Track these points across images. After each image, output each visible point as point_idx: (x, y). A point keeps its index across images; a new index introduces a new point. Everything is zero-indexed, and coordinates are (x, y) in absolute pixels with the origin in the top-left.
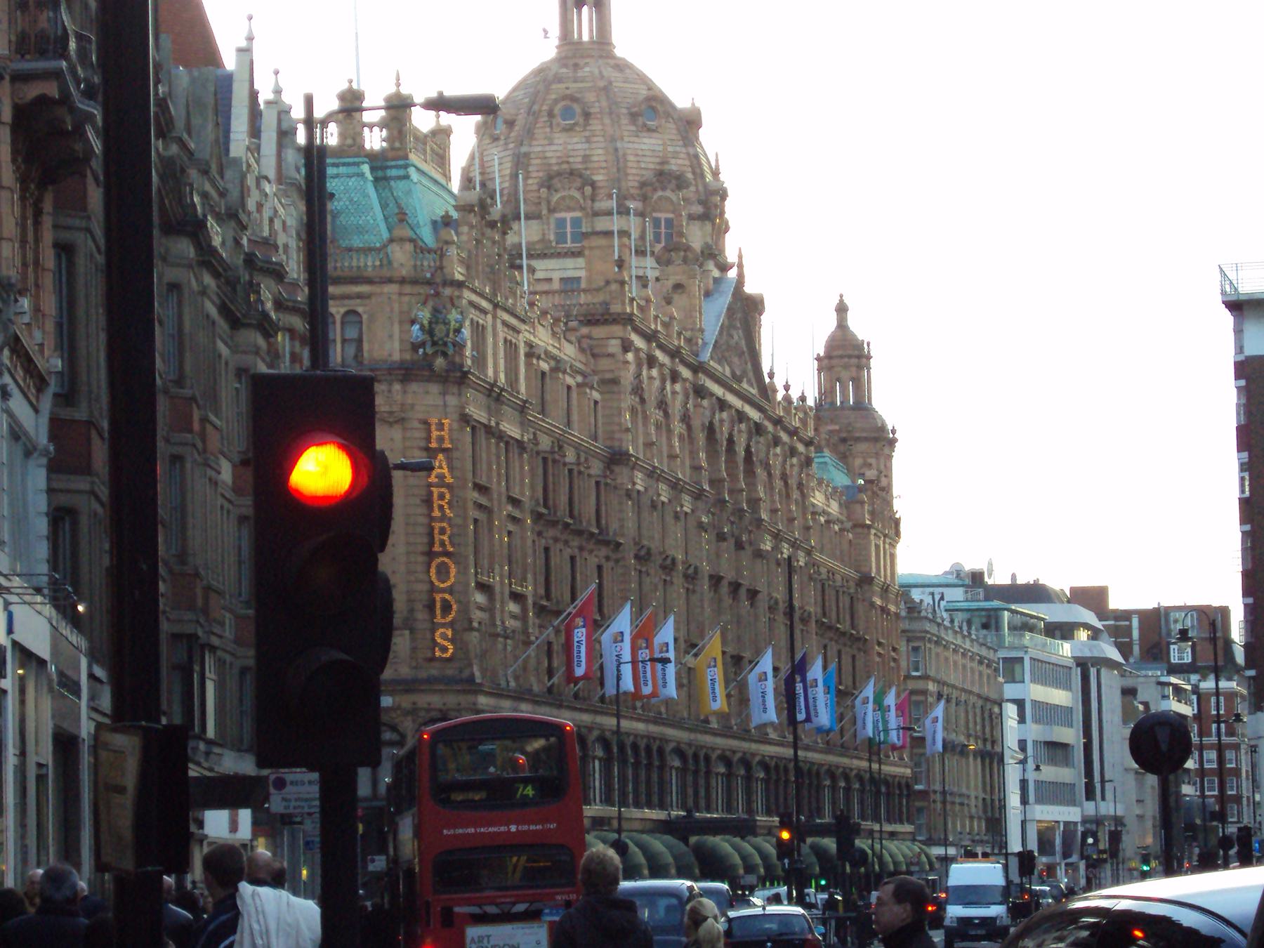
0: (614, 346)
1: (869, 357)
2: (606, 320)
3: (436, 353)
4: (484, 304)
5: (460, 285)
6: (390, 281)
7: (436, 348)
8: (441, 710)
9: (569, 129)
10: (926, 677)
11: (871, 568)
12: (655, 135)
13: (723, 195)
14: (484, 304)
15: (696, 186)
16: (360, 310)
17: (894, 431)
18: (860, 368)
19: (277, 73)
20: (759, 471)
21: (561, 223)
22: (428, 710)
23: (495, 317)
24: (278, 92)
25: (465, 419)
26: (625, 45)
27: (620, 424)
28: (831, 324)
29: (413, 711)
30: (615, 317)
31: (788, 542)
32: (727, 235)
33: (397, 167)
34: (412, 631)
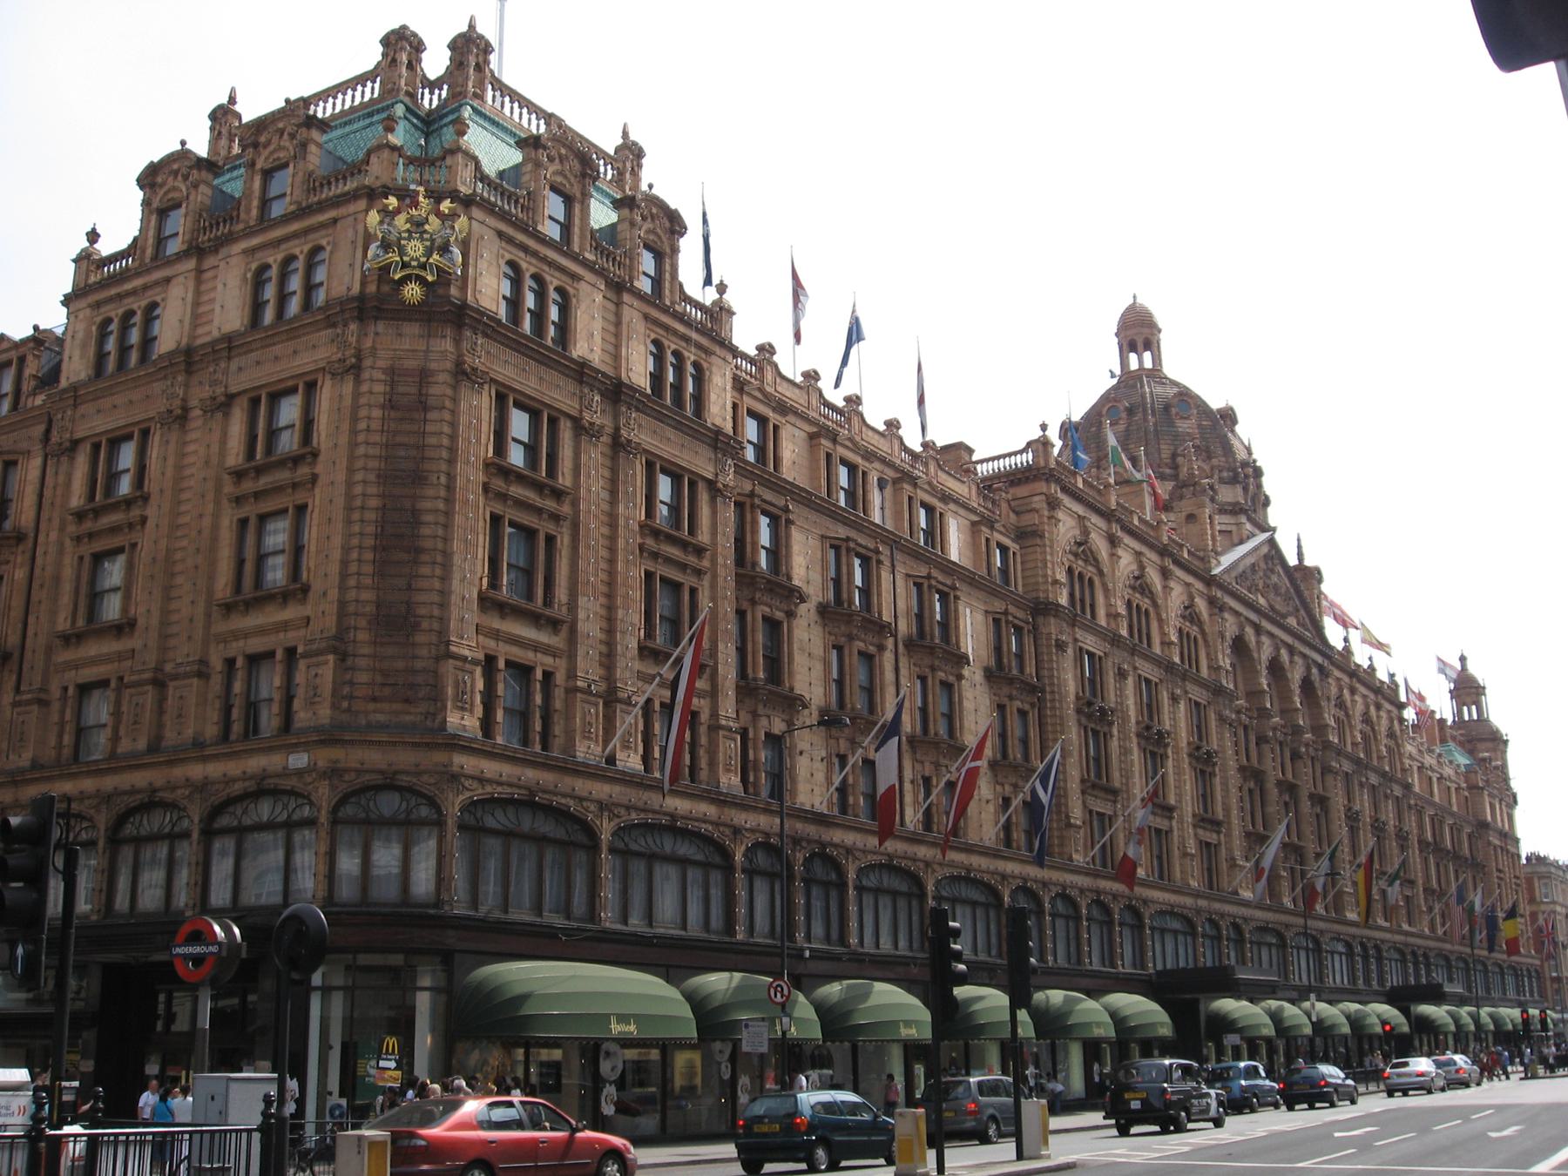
0: (1039, 502)
2: (1027, 478)
3: (405, 280)
7: (407, 272)
8: (381, 772)
10: (1554, 902)
13: (1258, 473)
16: (324, 242)
20: (1324, 703)
22: (357, 771)
25: (463, 374)
26: (1171, 369)
27: (1045, 576)
29: (334, 772)
30: (1035, 473)
33: (452, 111)
34: (343, 657)
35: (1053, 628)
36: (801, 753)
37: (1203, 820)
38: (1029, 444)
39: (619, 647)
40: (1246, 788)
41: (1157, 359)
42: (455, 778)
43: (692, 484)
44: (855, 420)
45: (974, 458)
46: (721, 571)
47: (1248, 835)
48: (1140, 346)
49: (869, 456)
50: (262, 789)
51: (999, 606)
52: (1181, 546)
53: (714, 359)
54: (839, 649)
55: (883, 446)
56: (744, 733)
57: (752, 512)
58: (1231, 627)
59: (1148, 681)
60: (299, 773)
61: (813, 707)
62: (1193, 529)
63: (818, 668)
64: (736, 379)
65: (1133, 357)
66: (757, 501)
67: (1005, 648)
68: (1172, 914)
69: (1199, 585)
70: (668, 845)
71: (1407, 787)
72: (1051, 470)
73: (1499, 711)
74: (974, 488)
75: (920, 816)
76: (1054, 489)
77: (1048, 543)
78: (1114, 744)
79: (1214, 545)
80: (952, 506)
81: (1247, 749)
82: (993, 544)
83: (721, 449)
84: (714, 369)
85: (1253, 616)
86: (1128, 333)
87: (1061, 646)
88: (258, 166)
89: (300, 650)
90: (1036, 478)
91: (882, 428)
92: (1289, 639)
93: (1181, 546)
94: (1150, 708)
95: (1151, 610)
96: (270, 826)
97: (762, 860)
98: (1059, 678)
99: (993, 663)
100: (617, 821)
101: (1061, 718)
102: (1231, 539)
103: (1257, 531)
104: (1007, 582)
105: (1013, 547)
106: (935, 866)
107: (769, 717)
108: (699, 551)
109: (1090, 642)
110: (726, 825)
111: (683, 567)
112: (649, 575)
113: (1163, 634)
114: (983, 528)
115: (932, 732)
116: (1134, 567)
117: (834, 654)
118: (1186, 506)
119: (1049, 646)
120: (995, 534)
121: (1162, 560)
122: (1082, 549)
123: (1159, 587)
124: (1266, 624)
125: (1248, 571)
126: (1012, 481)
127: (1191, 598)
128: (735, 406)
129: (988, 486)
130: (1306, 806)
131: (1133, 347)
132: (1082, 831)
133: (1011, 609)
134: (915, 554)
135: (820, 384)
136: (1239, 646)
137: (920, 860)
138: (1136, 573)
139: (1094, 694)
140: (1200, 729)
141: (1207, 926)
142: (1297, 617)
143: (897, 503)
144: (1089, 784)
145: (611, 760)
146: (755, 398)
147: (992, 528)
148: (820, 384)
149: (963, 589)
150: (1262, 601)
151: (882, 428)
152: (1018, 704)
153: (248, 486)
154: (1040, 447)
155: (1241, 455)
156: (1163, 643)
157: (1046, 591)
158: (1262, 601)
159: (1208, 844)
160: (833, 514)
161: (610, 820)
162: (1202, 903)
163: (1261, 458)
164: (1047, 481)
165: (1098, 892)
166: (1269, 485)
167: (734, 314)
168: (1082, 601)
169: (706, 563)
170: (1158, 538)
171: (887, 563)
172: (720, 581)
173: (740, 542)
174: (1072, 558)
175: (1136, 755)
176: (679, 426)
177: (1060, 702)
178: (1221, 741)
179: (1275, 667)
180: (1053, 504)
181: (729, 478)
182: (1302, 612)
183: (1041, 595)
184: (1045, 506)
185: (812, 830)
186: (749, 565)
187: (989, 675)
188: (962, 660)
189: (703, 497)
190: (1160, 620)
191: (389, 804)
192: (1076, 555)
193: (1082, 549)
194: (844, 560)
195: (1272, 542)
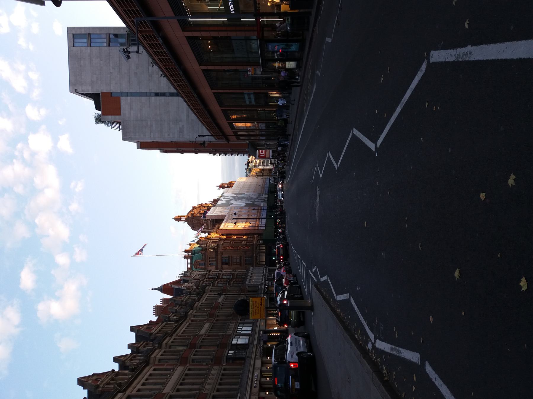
4: (209, 241)
5: (207, 245)
6: (206, 254)
9: (194, 221)
14: (209, 241)
19: (176, 277)
21: (205, 222)
23: (211, 239)
24: (179, 277)
25: (222, 245)
42: (256, 244)
50: (256, 259)
60: (255, 255)
88: (199, 267)
89: (245, 256)
96: (259, 258)
131: (181, 219)
153: (230, 264)
191: (258, 248)
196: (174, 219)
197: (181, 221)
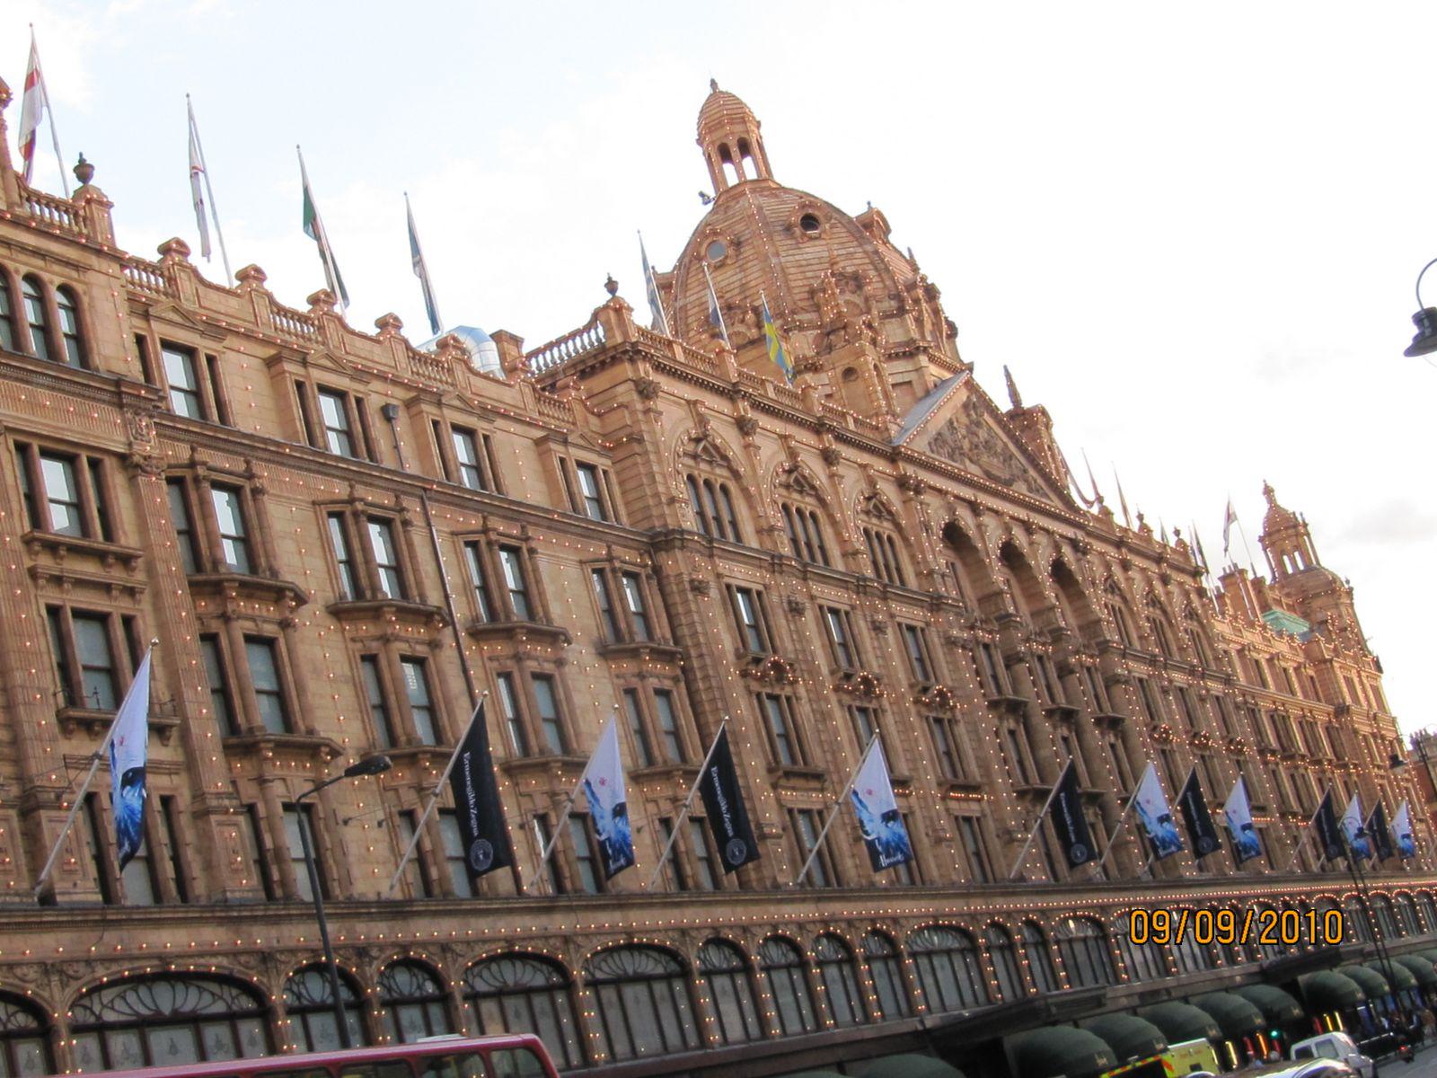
0: (626, 393)
1: (1305, 525)
2: (603, 363)
11: (1344, 700)
12: (817, 243)
13: (932, 293)
15: (883, 281)
17: (1348, 582)
18: (1298, 535)
20: (1089, 591)
26: (785, 175)
27: (657, 495)
28: (1263, 508)
30: (612, 353)
31: (1180, 669)
32: (959, 341)
35: (675, 563)
36: (346, 822)
37: (954, 788)
38: (596, 316)
39: (26, 727)
40: (1004, 732)
41: (763, 164)
43: (95, 465)
44: (331, 328)
45: (526, 349)
46: (165, 584)
47: (1022, 794)
48: (735, 151)
49: (361, 374)
51: (598, 550)
52: (844, 415)
53: (91, 277)
54: (371, 659)
55: (379, 357)
56: (251, 810)
57: (198, 488)
58: (937, 515)
59: (835, 612)
61: (351, 752)
62: (857, 387)
63: (347, 691)
64: (132, 299)
65: (728, 168)
66: (201, 471)
67: (618, 609)
68: (511, 956)
69: (881, 465)
70: (166, 999)
71: (1228, 681)
72: (634, 345)
73: (1333, 556)
74: (527, 391)
75: (544, 871)
76: (644, 369)
77: (650, 448)
78: (804, 709)
79: (889, 405)
80: (500, 423)
81: (995, 677)
82: (572, 465)
83: (130, 406)
84: (96, 292)
85: (967, 493)
86: (718, 135)
87: (699, 588)
90: (615, 360)
91: (373, 331)
92: (1022, 514)
93: (844, 415)
94: (849, 646)
95: (819, 512)
97: (316, 989)
98: (705, 634)
99: (607, 631)
100: (74, 985)
101: (721, 688)
102: (914, 394)
103: (947, 375)
104: (604, 516)
105: (602, 463)
106: (580, 940)
107: (284, 780)
108: (126, 560)
109: (740, 574)
110: (245, 952)
111: (106, 588)
112: (54, 612)
113: (842, 541)
114: (553, 446)
115: (536, 749)
116: (782, 457)
117: (366, 672)
118: (841, 359)
119: (682, 592)
120: (572, 450)
121: (821, 441)
122: (704, 447)
123: (824, 479)
124: (984, 499)
125: (947, 433)
126: (583, 372)
127: (872, 483)
128: (140, 340)
129: (549, 384)
130: (1095, 737)
131: (725, 155)
132: (784, 841)
133: (618, 551)
134: (457, 499)
135: (267, 285)
136: (954, 535)
137: (555, 936)
138: (787, 466)
139: (762, 647)
140: (924, 662)
141: (992, 934)
142: (1026, 481)
143: (418, 435)
144: (780, 773)
145: (47, 900)
146: (170, 322)
147: (565, 442)
148: (267, 285)
149: (539, 536)
150: (973, 469)
151: (373, 331)
152: (653, 682)
154: (612, 314)
155: (903, 274)
156: (844, 555)
157: (663, 516)
158: (974, 469)
159: (968, 820)
160: (321, 464)
161: (64, 986)
162: (978, 905)
163: (931, 271)
164: (632, 360)
165: (825, 922)
166: (950, 306)
167: (109, 205)
168: (718, 519)
169: (140, 576)
170: (809, 411)
171: (418, 521)
172: (168, 601)
173: (189, 534)
174: (691, 462)
175: (839, 719)
176: (57, 385)
177: (715, 667)
178: (955, 672)
179: (1010, 555)
180: (646, 391)
181: (149, 446)
182: (1032, 472)
183: (657, 523)
184: (635, 396)
185: (380, 931)
186: (208, 566)
187: (605, 653)
188: (555, 637)
189: (117, 480)
190: (834, 523)
192: (695, 457)
193: (704, 447)
194: (352, 530)
195: (971, 385)
196: (709, 91)
197: (709, 159)
